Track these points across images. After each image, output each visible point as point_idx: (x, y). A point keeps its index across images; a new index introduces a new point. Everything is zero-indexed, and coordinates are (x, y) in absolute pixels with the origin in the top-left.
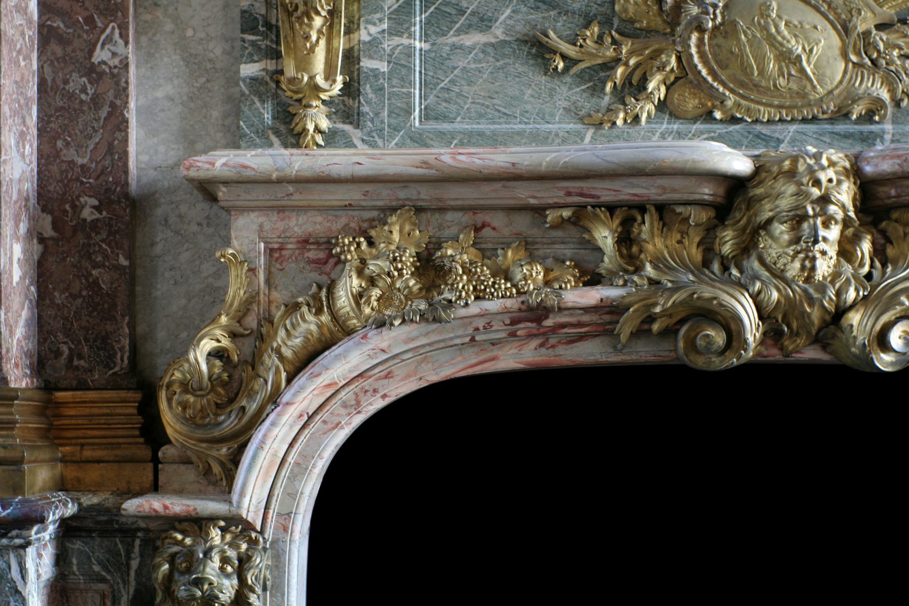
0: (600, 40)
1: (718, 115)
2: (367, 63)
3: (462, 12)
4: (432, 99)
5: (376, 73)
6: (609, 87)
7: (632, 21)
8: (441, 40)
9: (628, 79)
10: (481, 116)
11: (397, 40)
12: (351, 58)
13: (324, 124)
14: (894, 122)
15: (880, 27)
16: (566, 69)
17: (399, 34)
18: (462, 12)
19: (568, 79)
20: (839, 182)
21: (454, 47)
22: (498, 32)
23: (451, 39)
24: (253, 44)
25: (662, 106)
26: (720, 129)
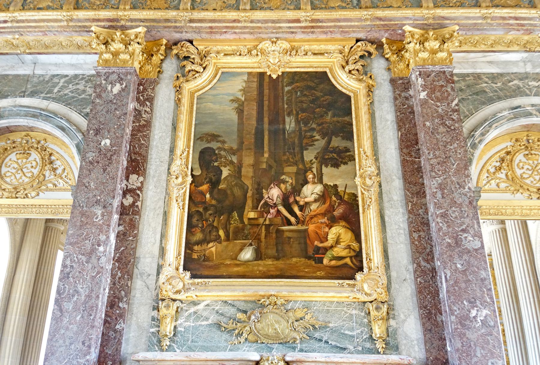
0: (233, 324)
1: (259, 342)
2: (179, 329)
3: (202, 317)
4: (194, 337)
5: (181, 331)
6: (234, 335)
7: (240, 319)
8: (197, 323)
9: (239, 333)
10: (205, 342)
11: (186, 323)
12: (175, 327)
13: (168, 343)
14: (300, 344)
15: (296, 321)
16: (225, 330)
17: (187, 322)
18: (202, 317)
19: (225, 333)
20: (278, 362)
21: (200, 325)
22: (210, 322)
23: (199, 323)
24: (154, 324)
25: (246, 339)
26: (260, 345)
